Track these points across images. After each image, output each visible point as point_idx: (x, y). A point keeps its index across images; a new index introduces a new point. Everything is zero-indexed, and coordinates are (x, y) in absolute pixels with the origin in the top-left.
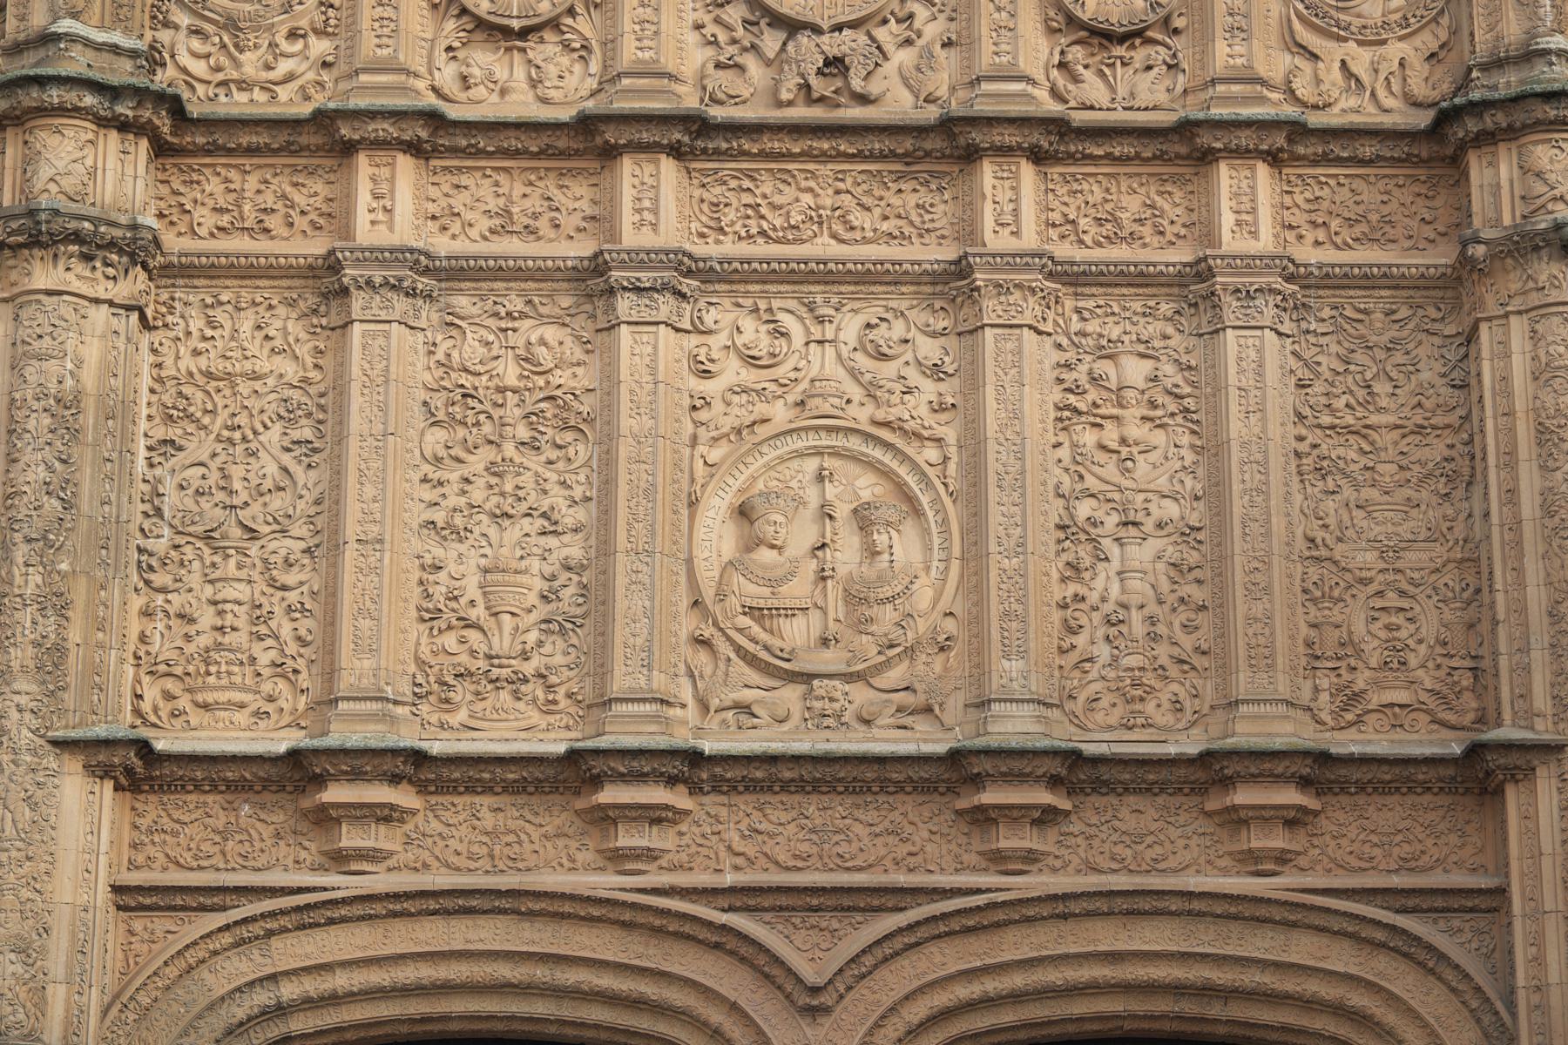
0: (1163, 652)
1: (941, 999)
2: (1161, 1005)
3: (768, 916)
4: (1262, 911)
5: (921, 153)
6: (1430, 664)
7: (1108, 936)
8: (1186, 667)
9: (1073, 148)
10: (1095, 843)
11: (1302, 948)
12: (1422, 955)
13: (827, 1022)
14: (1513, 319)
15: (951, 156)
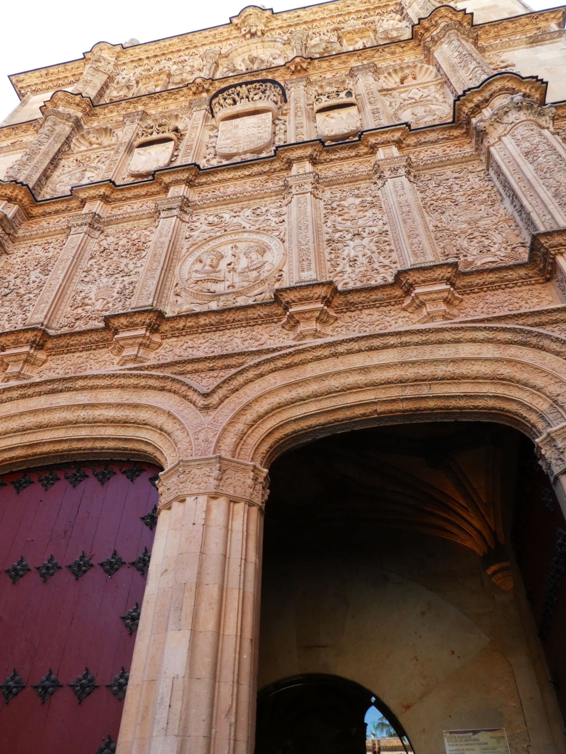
0: (376, 266)
1: (275, 400)
2: (395, 393)
3: (189, 376)
4: (440, 336)
5: (272, 170)
6: (503, 249)
7: (358, 361)
8: (387, 268)
9: (325, 158)
10: (351, 328)
11: (466, 350)
12: (534, 340)
13: (213, 413)
14: (503, 138)
15: (282, 170)
